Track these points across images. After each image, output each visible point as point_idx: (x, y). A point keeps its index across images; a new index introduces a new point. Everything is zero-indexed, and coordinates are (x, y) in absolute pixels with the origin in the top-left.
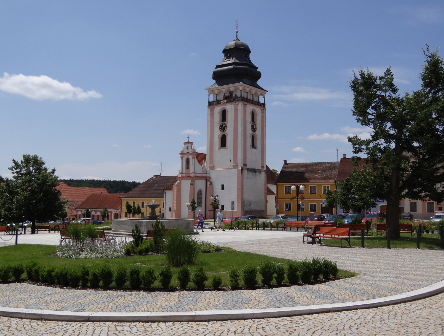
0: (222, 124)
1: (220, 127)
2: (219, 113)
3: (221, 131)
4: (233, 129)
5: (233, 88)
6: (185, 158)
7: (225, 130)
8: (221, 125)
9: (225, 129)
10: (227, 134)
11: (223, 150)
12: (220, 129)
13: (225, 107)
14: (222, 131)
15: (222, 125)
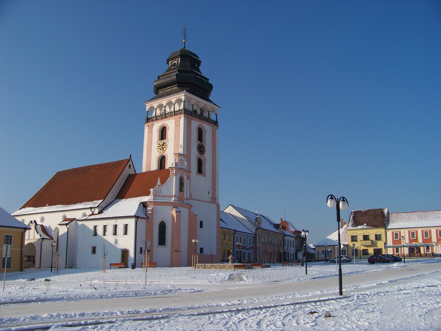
0: (200, 144)
1: (198, 147)
2: (196, 128)
3: (199, 152)
4: (211, 155)
5: (210, 108)
6: (179, 175)
7: (204, 153)
8: (199, 145)
9: (204, 152)
10: (205, 159)
11: (200, 177)
12: (198, 149)
13: (203, 125)
14: (200, 154)
15: (200, 145)
